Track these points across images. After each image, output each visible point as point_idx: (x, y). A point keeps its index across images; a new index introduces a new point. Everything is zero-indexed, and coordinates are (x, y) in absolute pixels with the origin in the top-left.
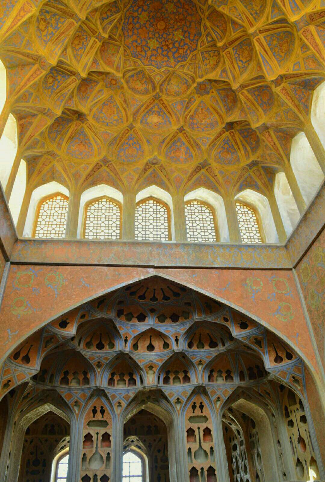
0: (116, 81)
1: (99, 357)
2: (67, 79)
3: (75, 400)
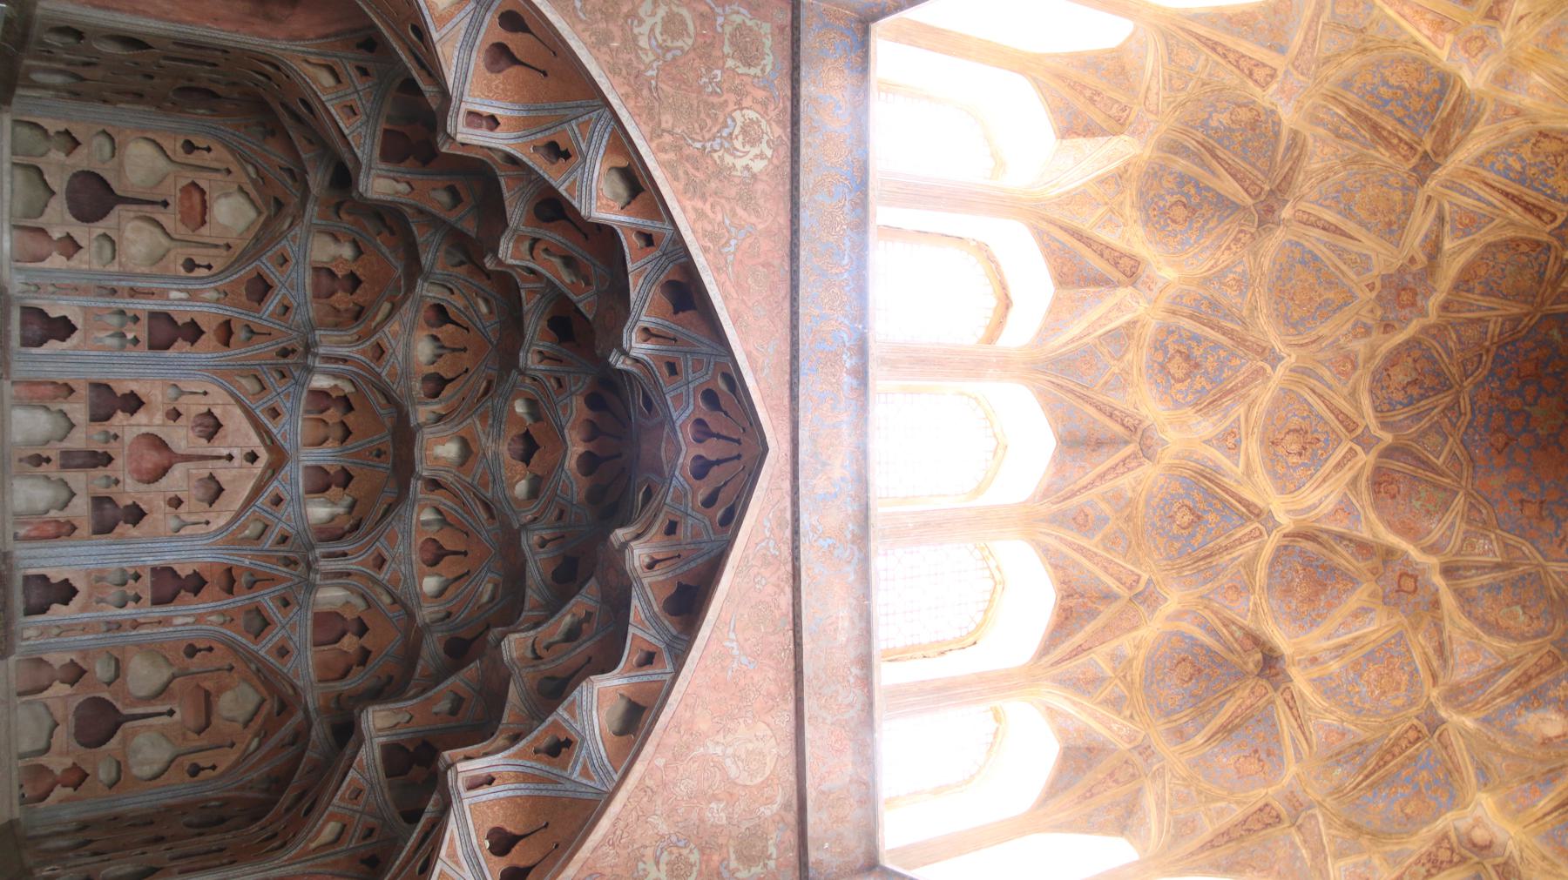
0: (1415, 578)
2: (1235, 527)
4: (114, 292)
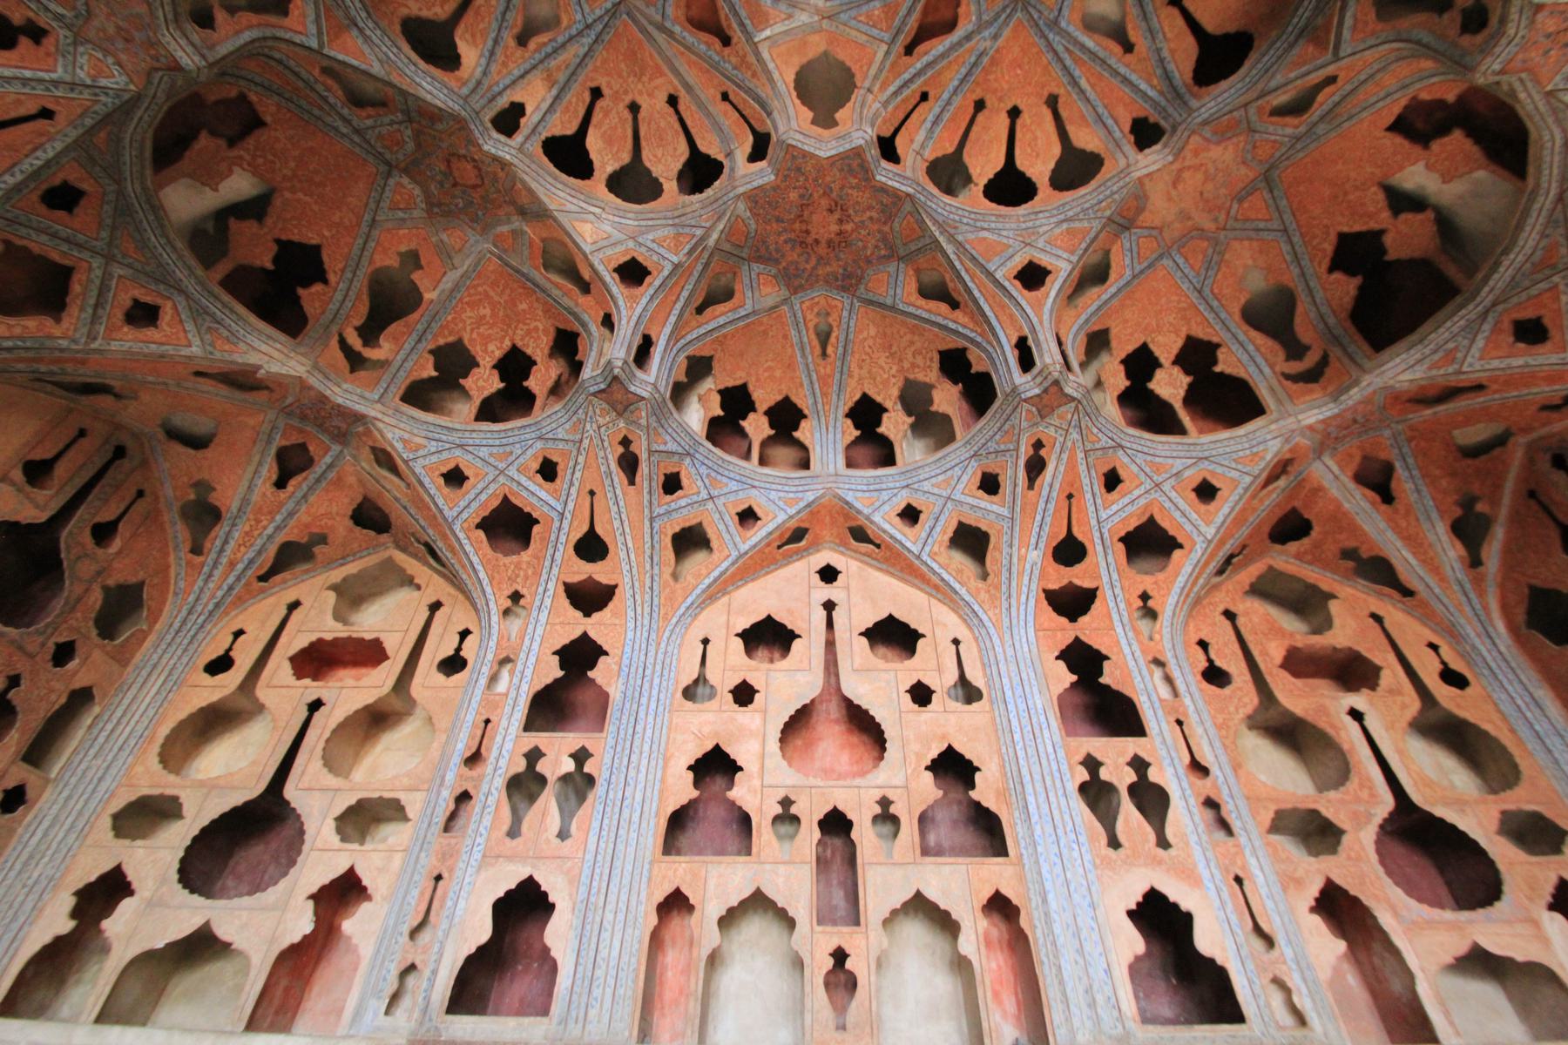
4: (464, 797)
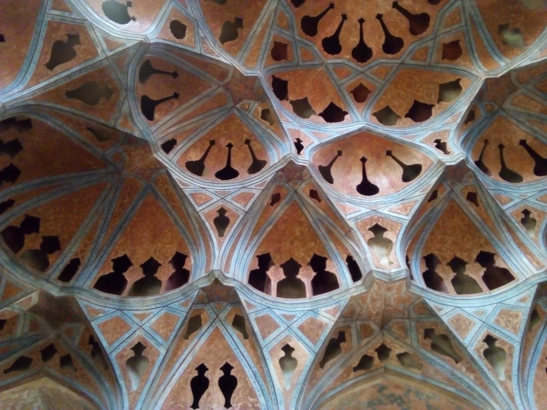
1: (223, 195)
3: (134, 340)
